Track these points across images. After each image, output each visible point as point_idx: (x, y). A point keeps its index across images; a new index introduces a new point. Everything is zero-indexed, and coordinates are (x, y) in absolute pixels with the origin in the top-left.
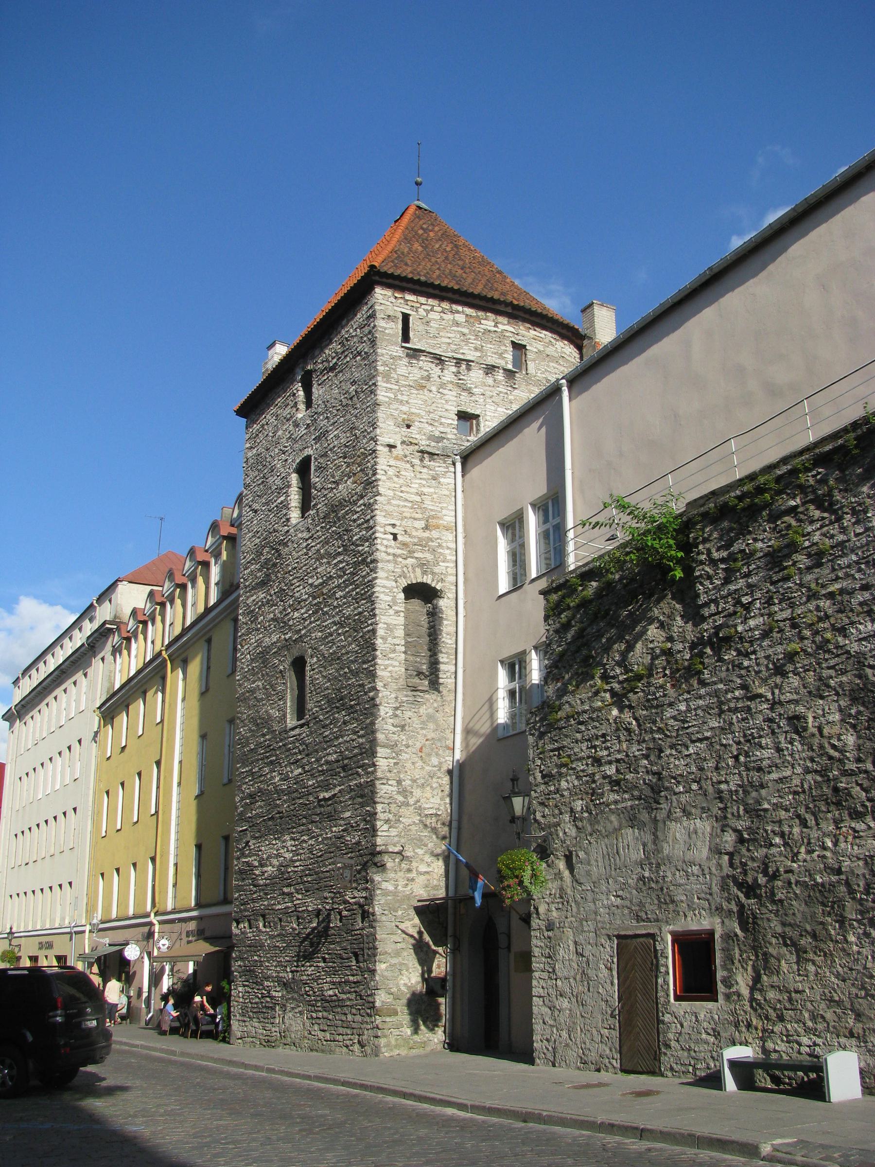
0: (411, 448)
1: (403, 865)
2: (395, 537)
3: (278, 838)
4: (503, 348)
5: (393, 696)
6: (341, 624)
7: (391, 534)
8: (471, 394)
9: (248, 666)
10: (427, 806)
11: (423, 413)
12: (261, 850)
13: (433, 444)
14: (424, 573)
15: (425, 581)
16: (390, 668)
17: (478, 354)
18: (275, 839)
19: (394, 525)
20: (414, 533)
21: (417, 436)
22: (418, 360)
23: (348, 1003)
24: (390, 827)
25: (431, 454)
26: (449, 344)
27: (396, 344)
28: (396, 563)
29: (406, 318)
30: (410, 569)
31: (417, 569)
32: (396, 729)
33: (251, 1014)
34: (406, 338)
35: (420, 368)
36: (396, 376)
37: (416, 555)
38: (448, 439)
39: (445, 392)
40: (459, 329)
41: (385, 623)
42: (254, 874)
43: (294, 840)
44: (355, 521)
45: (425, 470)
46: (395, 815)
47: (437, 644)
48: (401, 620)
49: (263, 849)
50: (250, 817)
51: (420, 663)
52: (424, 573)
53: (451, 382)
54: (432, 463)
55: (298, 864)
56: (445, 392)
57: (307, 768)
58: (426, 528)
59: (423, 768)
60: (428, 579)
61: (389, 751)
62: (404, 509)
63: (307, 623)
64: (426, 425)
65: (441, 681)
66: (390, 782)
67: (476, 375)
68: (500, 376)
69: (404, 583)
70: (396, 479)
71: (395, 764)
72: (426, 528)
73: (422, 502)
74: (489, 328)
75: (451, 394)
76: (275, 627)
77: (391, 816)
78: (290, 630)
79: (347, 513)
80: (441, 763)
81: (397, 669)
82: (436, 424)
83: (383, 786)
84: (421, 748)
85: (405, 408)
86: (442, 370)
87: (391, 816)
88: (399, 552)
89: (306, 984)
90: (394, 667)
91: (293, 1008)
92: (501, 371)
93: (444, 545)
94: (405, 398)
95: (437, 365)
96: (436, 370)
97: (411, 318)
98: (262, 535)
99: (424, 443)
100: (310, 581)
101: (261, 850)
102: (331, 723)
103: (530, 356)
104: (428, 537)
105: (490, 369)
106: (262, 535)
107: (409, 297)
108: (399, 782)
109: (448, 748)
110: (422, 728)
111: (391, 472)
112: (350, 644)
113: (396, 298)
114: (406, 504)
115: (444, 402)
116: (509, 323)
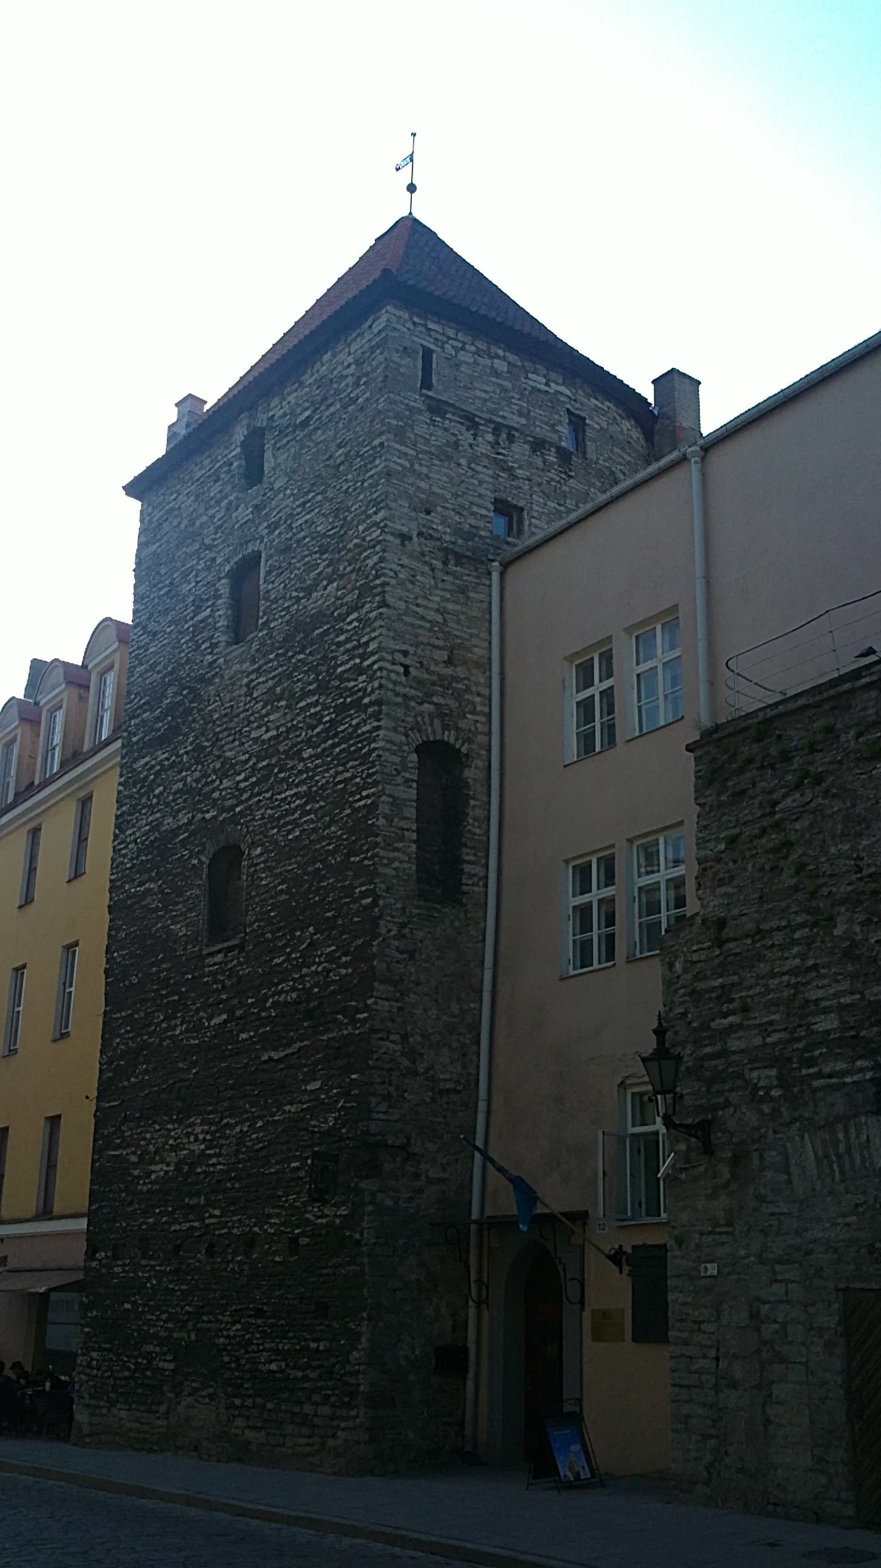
0: (431, 543)
1: (407, 1167)
2: (407, 673)
3: (179, 1121)
4: (557, 417)
5: (399, 905)
6: (310, 797)
7: (402, 665)
9: (132, 859)
10: (442, 1077)
11: (449, 496)
12: (144, 1139)
13: (460, 541)
14: (445, 727)
16: (396, 864)
17: (523, 421)
18: (173, 1122)
19: (405, 653)
21: (440, 528)
23: (306, 1385)
24: (390, 1107)
26: (485, 400)
28: (407, 707)
33: (113, 1396)
34: (427, 383)
35: (446, 430)
37: (435, 699)
38: (481, 537)
39: (479, 469)
40: (499, 381)
41: (390, 796)
42: (131, 1175)
43: (210, 1124)
46: (398, 1088)
48: (413, 793)
49: (148, 1136)
50: (124, 1087)
52: (445, 727)
54: (458, 569)
55: (214, 1160)
57: (239, 1013)
58: (449, 662)
59: (438, 1018)
60: (450, 737)
62: (420, 631)
63: (245, 796)
64: (452, 513)
66: (392, 1037)
67: (520, 450)
69: (417, 738)
70: (410, 586)
71: (399, 1009)
72: (449, 662)
74: (539, 386)
76: (185, 801)
77: (392, 1089)
79: (326, 633)
81: (407, 866)
82: (465, 513)
83: (382, 1043)
87: (392, 1089)
88: (413, 692)
89: (225, 1349)
91: (196, 1390)
93: (473, 689)
94: (425, 470)
97: (434, 356)
98: (165, 667)
99: (447, 538)
100: (254, 735)
101: (144, 1139)
102: (287, 945)
104: (452, 676)
105: (538, 446)
106: (165, 667)
107: (431, 326)
108: (405, 1037)
110: (438, 958)
112: (328, 826)
113: (414, 324)
114: (423, 623)
115: (476, 482)
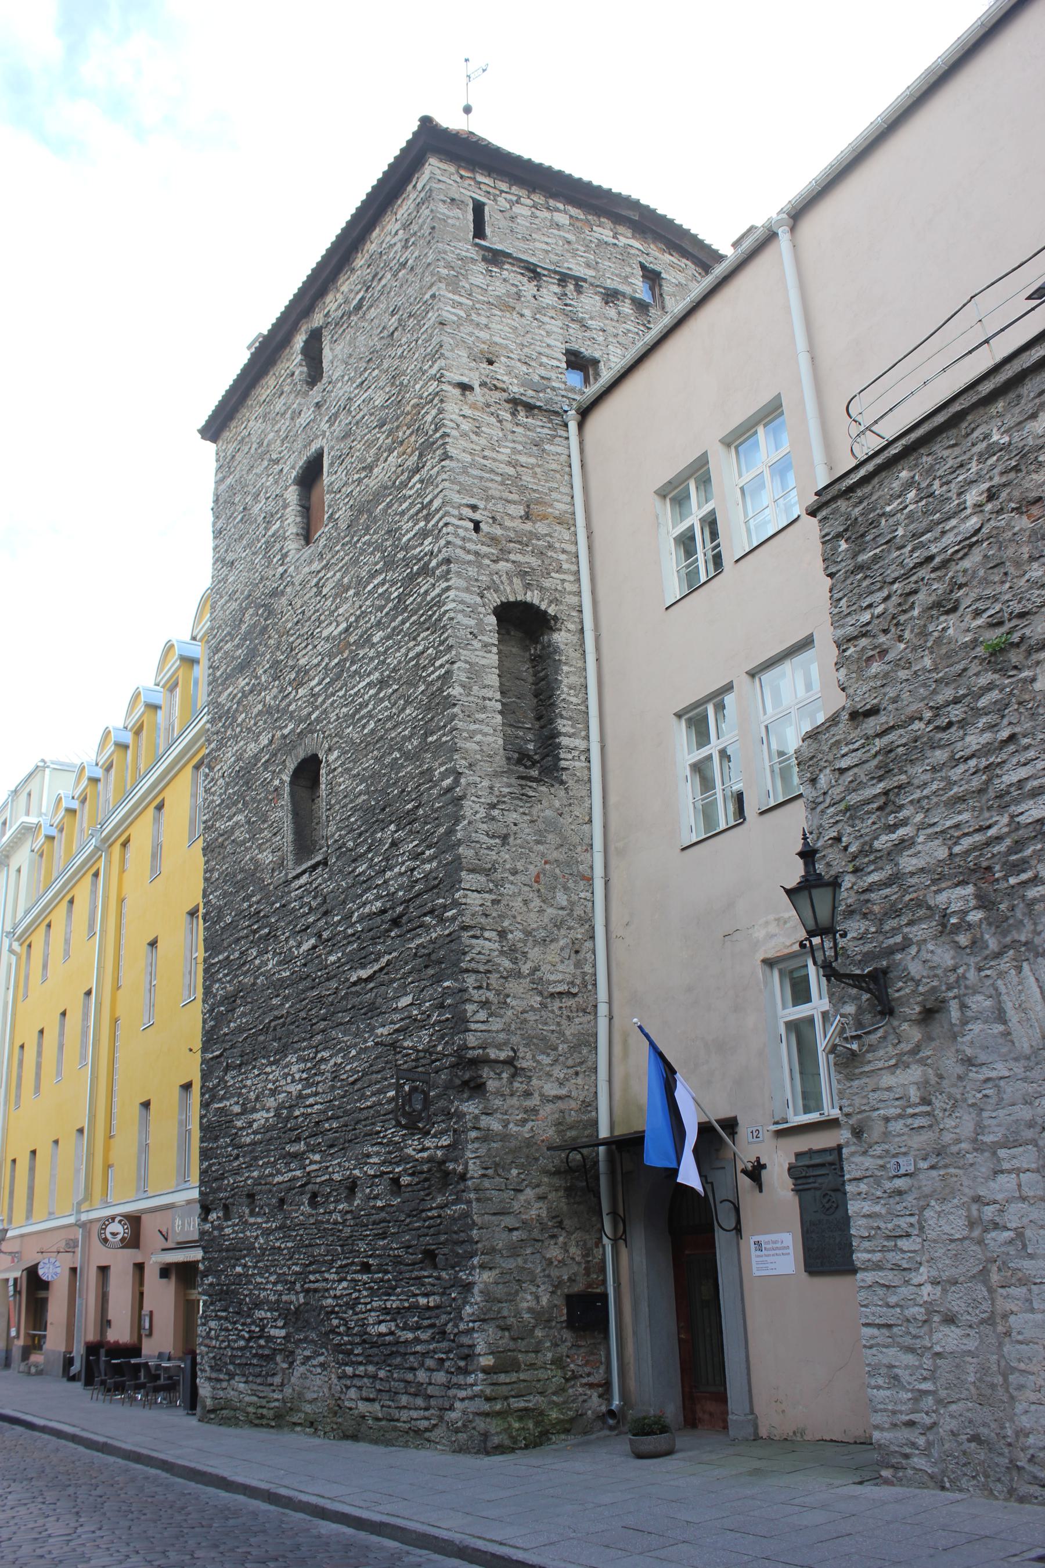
0: (497, 395)
1: (516, 1085)
2: (477, 528)
3: (276, 1062)
4: (628, 269)
5: (486, 783)
6: (383, 683)
7: (471, 520)
8: (586, 327)
9: (220, 795)
10: (552, 978)
11: (513, 346)
12: (245, 1086)
13: (530, 393)
14: (528, 586)
15: (529, 599)
16: (478, 738)
17: (592, 273)
18: (271, 1064)
19: (474, 508)
20: (508, 523)
21: (505, 378)
22: (501, 268)
23: (418, 1348)
24: (491, 1015)
25: (530, 408)
26: (547, 252)
27: (466, 240)
28: (480, 566)
29: (479, 209)
30: (504, 578)
31: (515, 580)
32: (492, 841)
33: (231, 1367)
34: (479, 232)
35: (505, 280)
36: (467, 286)
37: (512, 557)
38: (553, 389)
39: (546, 319)
40: (562, 233)
41: (466, 662)
42: (235, 1127)
43: (305, 1061)
44: (403, 513)
45: (519, 430)
46: (498, 993)
47: (553, 704)
48: (493, 659)
49: (249, 1083)
50: (226, 1034)
51: (522, 738)
52: (528, 586)
53: (554, 308)
54: (529, 420)
55: (311, 1100)
56: (546, 319)
57: (325, 935)
58: (527, 517)
59: (541, 911)
60: (533, 597)
61: (483, 879)
62: (490, 485)
63: (320, 700)
64: (519, 364)
65: (563, 764)
66: (487, 934)
67: (589, 303)
68: (627, 308)
69: (495, 599)
70: (474, 437)
71: (494, 902)
72: (527, 517)
73: (518, 477)
74: (606, 239)
75: (555, 325)
76: (265, 722)
77: (491, 995)
78: (291, 718)
79: (389, 506)
80: (572, 904)
81: (490, 739)
82: (533, 364)
83: (474, 941)
84: (538, 876)
85: (483, 335)
86: (539, 288)
87: (491, 995)
88: (485, 549)
89: (333, 1312)
90: (486, 735)
91: (308, 1358)
92: (628, 301)
93: (557, 545)
94: (483, 320)
95: (530, 280)
96: (529, 288)
97: (487, 209)
98: (242, 593)
99: (515, 389)
100: (325, 633)
101: (245, 1086)
102: (369, 850)
103: (667, 288)
104: (530, 532)
105: (611, 296)
106: (242, 593)
107: (480, 178)
108: (502, 934)
109: (584, 878)
110: (538, 842)
111: (466, 426)
112: (404, 709)
113: (462, 177)
114: (492, 476)
115: (544, 333)
116: (633, 237)
